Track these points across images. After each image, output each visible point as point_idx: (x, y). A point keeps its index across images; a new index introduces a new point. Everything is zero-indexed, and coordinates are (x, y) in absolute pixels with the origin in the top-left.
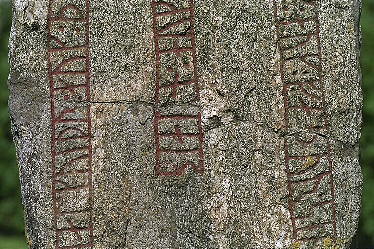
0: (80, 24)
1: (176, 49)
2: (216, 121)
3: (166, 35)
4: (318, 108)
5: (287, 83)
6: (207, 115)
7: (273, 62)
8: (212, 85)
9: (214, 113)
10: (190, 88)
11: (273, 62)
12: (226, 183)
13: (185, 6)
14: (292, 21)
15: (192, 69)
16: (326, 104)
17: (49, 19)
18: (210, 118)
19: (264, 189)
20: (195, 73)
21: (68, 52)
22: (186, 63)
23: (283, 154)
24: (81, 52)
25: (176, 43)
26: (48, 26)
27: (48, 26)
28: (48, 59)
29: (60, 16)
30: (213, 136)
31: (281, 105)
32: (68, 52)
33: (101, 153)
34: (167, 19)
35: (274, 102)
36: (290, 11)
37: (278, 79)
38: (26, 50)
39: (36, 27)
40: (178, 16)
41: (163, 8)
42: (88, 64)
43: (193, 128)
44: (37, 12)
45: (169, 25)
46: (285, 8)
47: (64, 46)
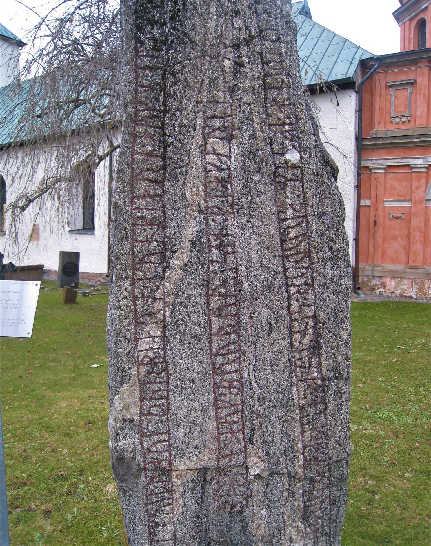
0: (163, 418)
1: (232, 432)
2: (258, 476)
3: (225, 423)
4: (324, 461)
5: (305, 447)
6: (252, 474)
7: (296, 434)
8: (256, 454)
9: (257, 472)
10: (241, 457)
11: (296, 434)
12: (264, 512)
13: (237, 402)
14: (309, 405)
15: (243, 444)
16: (330, 458)
17: (141, 414)
18: (254, 475)
19: (288, 514)
20: (245, 447)
21: (155, 438)
22: (239, 442)
23: (301, 491)
24: (163, 437)
25: (231, 429)
26: (140, 421)
27: (140, 421)
28: (141, 443)
29: (150, 413)
30: (255, 486)
31: (301, 462)
32: (155, 438)
33: (181, 502)
34: (226, 411)
35: (297, 461)
36: (309, 399)
37: (300, 445)
38: (125, 438)
39: (131, 421)
40: (233, 409)
41: (222, 404)
42: (170, 445)
43: (242, 481)
44: (132, 410)
45: (226, 416)
46: (305, 398)
47: (153, 433)
